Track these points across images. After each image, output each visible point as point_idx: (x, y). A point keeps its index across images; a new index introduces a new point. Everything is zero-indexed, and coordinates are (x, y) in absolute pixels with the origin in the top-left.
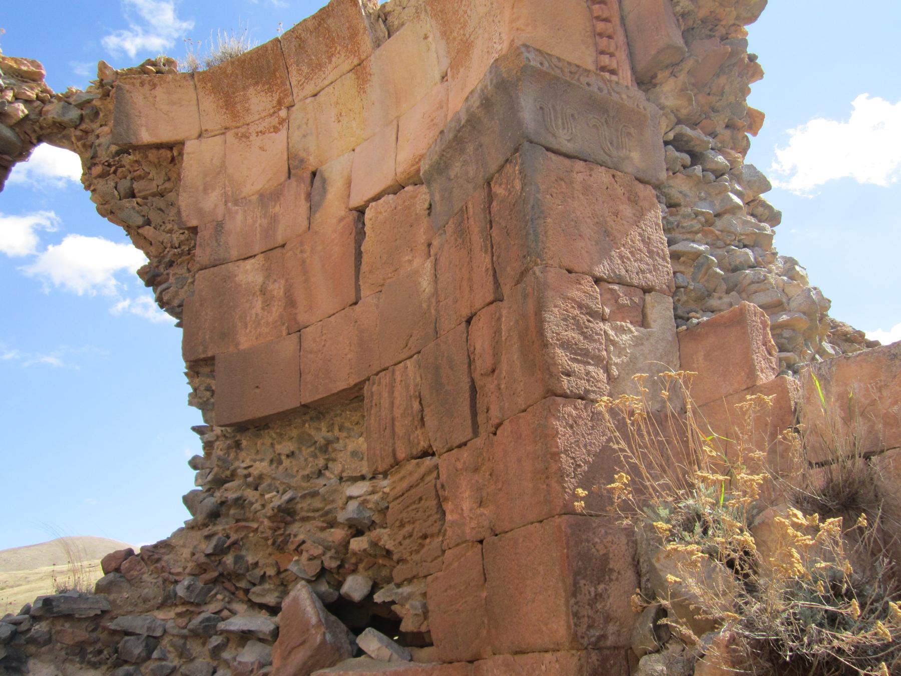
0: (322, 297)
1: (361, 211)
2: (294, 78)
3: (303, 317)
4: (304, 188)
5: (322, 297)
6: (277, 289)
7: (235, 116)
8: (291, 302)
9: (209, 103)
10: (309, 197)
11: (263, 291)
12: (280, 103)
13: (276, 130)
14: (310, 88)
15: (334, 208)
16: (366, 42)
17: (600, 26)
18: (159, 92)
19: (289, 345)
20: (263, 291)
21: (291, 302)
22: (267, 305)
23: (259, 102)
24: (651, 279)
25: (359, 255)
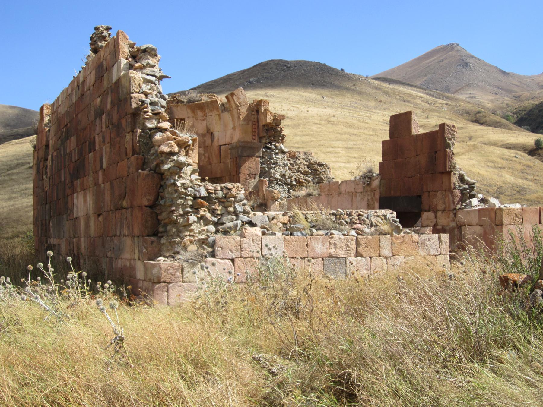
0: (215, 161)
1: (221, 146)
2: (207, 111)
3: (211, 162)
4: (210, 136)
5: (215, 161)
6: (206, 155)
7: (195, 115)
8: (209, 159)
9: (189, 111)
10: (211, 138)
11: (204, 155)
12: (204, 115)
13: (204, 121)
14: (210, 114)
15: (216, 144)
16: (220, 111)
17: (254, 130)
18: (179, 108)
19: (209, 167)
20: (204, 155)
21: (209, 159)
22: (205, 157)
23: (200, 113)
24: (256, 173)
25: (220, 155)
